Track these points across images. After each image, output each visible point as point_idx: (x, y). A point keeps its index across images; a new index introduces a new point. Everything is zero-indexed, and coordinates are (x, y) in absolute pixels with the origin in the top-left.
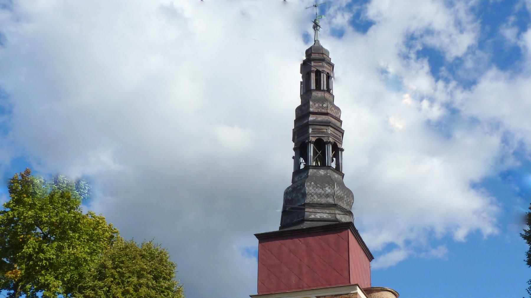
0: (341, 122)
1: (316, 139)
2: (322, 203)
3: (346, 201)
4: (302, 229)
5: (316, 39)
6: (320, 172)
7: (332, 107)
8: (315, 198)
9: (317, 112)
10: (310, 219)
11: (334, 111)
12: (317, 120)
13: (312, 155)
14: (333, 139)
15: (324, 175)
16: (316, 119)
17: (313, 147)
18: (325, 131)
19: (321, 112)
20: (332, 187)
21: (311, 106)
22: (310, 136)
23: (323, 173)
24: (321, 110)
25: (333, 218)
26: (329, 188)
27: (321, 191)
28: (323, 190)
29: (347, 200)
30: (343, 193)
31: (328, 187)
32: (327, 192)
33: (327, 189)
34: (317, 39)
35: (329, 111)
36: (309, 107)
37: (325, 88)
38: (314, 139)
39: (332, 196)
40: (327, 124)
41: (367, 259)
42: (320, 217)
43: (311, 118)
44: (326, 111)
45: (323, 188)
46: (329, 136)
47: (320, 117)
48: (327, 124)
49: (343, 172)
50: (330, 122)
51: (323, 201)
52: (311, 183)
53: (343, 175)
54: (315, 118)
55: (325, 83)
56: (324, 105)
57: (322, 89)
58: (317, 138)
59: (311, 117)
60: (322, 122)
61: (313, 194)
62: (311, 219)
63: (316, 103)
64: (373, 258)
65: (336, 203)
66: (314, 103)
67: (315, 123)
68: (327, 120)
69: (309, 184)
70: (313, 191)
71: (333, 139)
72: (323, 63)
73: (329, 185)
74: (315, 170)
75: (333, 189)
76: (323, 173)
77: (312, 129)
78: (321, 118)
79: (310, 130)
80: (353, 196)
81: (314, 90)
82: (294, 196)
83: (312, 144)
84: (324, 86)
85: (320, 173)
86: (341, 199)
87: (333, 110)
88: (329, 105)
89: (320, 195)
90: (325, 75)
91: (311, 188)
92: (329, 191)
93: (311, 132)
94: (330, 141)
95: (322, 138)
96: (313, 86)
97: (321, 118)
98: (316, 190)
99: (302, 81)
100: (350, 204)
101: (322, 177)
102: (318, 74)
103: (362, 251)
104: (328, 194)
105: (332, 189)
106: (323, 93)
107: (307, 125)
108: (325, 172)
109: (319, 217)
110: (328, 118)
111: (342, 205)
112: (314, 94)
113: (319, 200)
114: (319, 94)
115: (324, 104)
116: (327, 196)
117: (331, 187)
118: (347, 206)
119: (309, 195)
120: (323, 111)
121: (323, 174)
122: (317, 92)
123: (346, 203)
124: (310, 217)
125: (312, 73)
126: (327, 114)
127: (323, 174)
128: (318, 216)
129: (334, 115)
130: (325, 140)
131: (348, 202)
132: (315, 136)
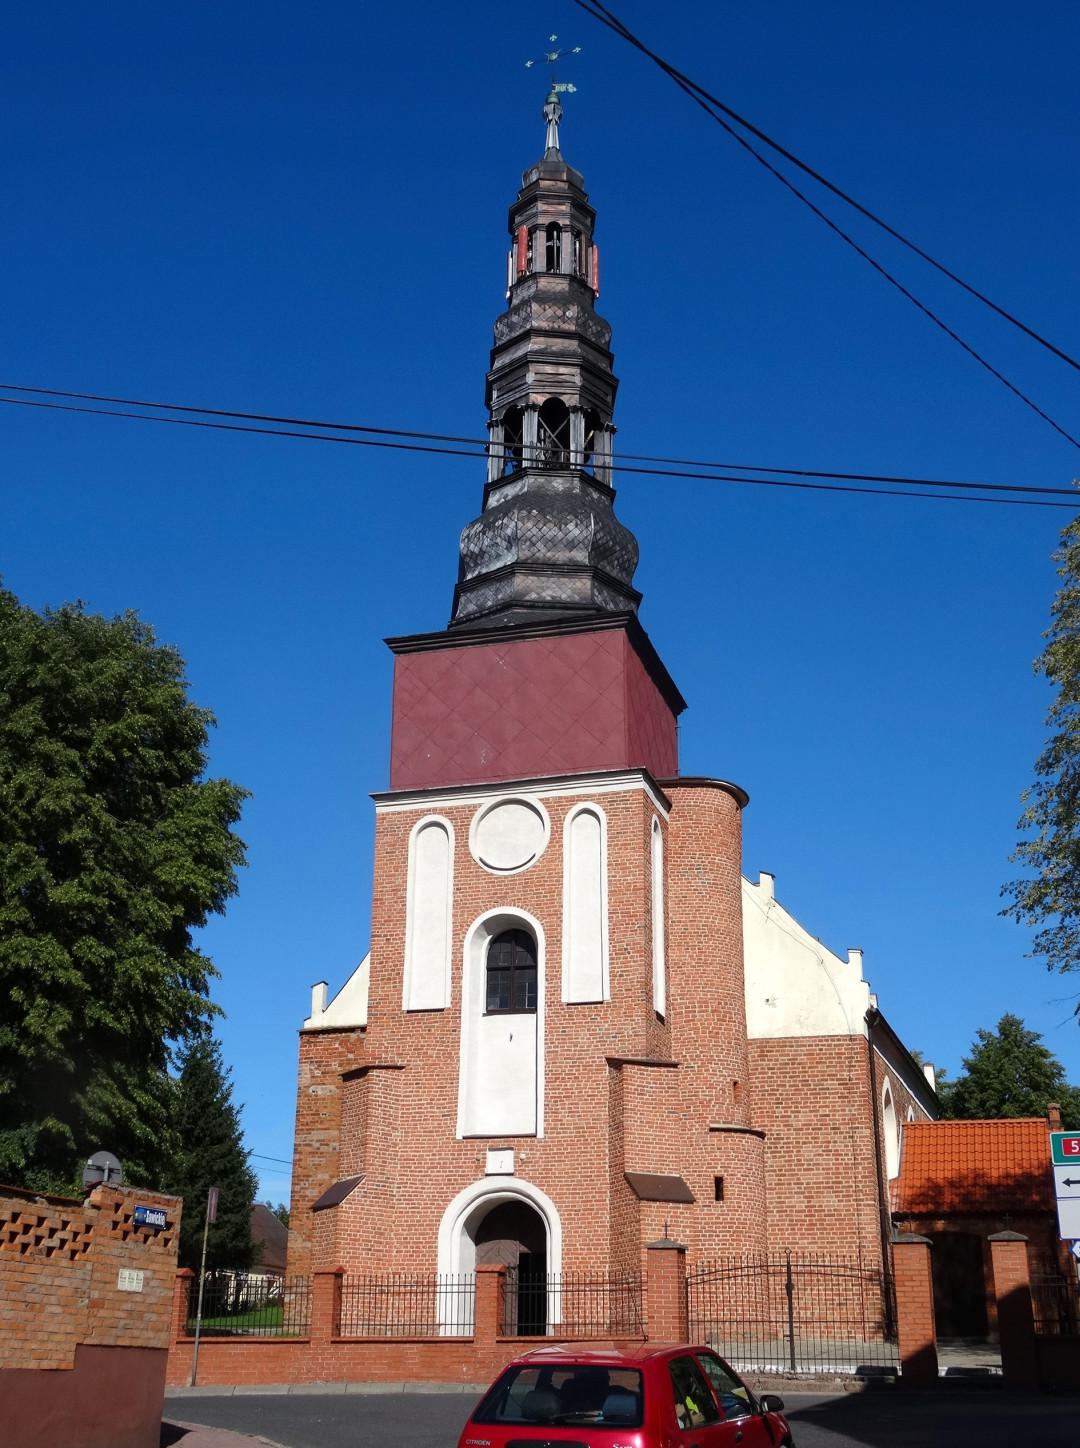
0: (610, 358)
2: (558, 563)
10: (526, 604)
23: (561, 488)
26: (576, 526)
28: (560, 529)
29: (622, 556)
30: (611, 539)
32: (570, 536)
33: (571, 526)
42: (553, 597)
45: (561, 523)
51: (562, 556)
52: (530, 512)
61: (534, 539)
70: (535, 531)
73: (576, 517)
74: (541, 480)
75: (587, 527)
76: (561, 488)
80: (636, 548)
82: (486, 543)
89: (552, 543)
92: (577, 532)
100: (629, 568)
108: (568, 485)
116: (571, 545)
117: (582, 523)
118: (621, 571)
119: (525, 542)
123: (619, 564)
124: (527, 598)
128: (547, 595)
131: (624, 562)
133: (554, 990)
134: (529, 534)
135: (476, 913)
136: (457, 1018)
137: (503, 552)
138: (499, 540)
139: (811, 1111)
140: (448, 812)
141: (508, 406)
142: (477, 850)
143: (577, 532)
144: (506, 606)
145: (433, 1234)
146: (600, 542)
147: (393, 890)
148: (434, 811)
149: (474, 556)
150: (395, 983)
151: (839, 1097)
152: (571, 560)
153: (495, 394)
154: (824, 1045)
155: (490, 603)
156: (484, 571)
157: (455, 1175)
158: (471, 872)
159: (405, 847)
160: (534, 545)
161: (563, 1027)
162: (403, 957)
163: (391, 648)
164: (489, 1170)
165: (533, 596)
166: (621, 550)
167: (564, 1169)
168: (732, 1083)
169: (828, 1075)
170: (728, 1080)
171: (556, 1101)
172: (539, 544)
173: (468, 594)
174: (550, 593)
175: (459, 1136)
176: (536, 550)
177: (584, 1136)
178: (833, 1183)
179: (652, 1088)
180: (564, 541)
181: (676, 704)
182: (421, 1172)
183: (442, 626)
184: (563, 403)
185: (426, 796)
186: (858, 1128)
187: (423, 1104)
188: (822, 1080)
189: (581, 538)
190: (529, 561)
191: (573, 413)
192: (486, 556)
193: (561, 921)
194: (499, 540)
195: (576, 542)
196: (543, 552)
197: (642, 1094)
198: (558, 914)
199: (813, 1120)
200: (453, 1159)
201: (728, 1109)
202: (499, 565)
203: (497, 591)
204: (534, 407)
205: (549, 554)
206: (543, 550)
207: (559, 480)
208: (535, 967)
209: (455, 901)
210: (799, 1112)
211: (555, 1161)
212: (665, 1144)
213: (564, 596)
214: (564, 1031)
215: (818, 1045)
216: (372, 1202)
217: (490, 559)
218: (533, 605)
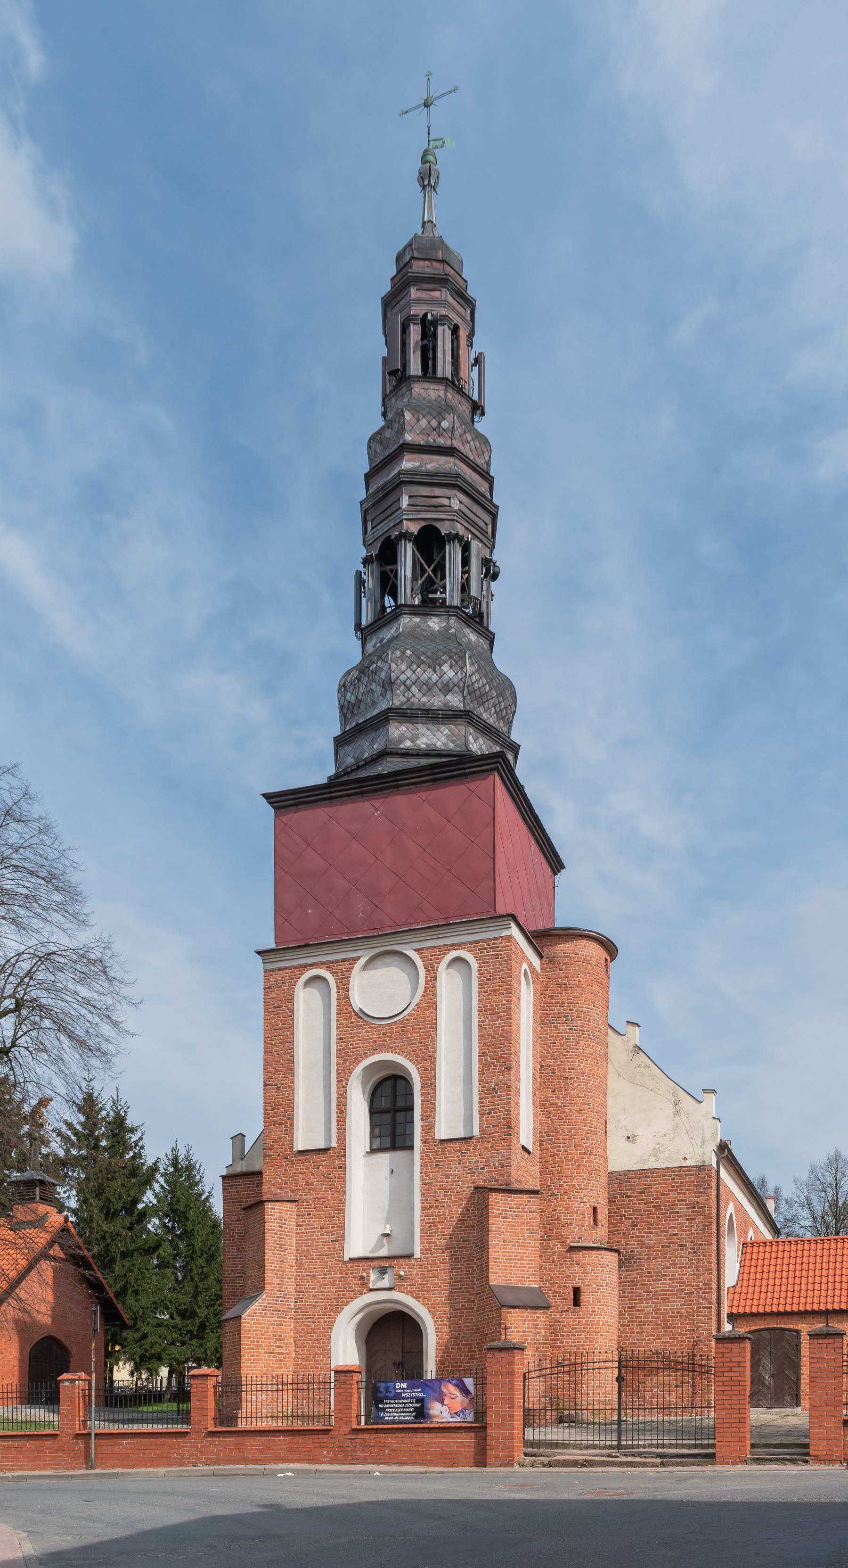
0: (490, 480)
1: (419, 527)
2: (433, 708)
3: (495, 706)
4: (380, 776)
5: (426, 219)
6: (431, 624)
7: (465, 433)
8: (414, 695)
9: (424, 444)
10: (400, 751)
11: (472, 443)
12: (423, 469)
13: (409, 573)
14: (466, 528)
15: (438, 631)
16: (420, 466)
17: (413, 551)
18: (445, 502)
19: (436, 445)
20: (460, 663)
21: (408, 427)
22: (404, 517)
23: (437, 628)
24: (434, 441)
25: (458, 749)
26: (451, 667)
27: (428, 675)
28: (435, 672)
29: (499, 703)
30: (487, 683)
31: (449, 662)
33: (445, 667)
34: (431, 219)
35: (456, 444)
36: (402, 431)
37: (448, 374)
38: (414, 528)
39: (459, 688)
40: (452, 482)
41: (549, 870)
42: (427, 745)
43: (408, 463)
44: (448, 443)
46: (455, 518)
47: (432, 461)
48: (452, 482)
49: (492, 628)
50: (458, 476)
51: (436, 701)
52: (403, 653)
53: (490, 638)
54: (417, 464)
55: (449, 358)
56: (443, 424)
57: (439, 374)
58: (423, 524)
59: (408, 461)
60: (436, 474)
62: (403, 751)
63: (421, 416)
64: (563, 867)
65: (468, 708)
66: (416, 416)
67: (417, 479)
68: (450, 468)
69: (398, 653)
70: (409, 673)
71: (466, 528)
72: (443, 289)
73: (451, 658)
74: (417, 620)
75: (462, 668)
76: (437, 628)
77: (410, 497)
78: (434, 463)
79: (405, 501)
80: (514, 694)
81: (418, 377)
83: (410, 541)
84: (444, 368)
85: (429, 627)
86: (481, 698)
87: (468, 442)
88: (457, 425)
89: (427, 687)
90: (448, 333)
91: (403, 667)
93: (408, 505)
94: (457, 534)
95: (438, 525)
96: (415, 367)
97: (434, 463)
98: (417, 672)
99: (386, 355)
100: (508, 716)
101: (432, 636)
102: (429, 328)
103: (533, 842)
104: (446, 685)
105: (458, 669)
106: (442, 388)
107: (397, 484)
109: (423, 746)
110: (455, 465)
111: (485, 716)
112: (418, 389)
113: (424, 699)
114: (431, 392)
115: (444, 419)
116: (446, 689)
117: (456, 663)
118: (498, 720)
119: (400, 686)
120: (441, 441)
121: (436, 629)
122: (426, 385)
123: (496, 713)
124: (402, 746)
125: (411, 325)
126: (450, 451)
127: (436, 629)
128: (422, 743)
129: (472, 458)
130: (444, 529)
131: (501, 710)
132: (419, 516)
133: (429, 1127)
134: (403, 677)
135: (357, 1061)
136: (342, 1156)
138: (374, 686)
139: (661, 1232)
140: (328, 965)
142: (358, 1001)
143: (451, 674)
144: (383, 754)
145: (326, 1339)
146: (476, 686)
147: (282, 1042)
150: (287, 1126)
151: (687, 1219)
152: (446, 704)
154: (676, 1175)
155: (366, 755)
156: (361, 721)
157: (344, 1291)
158: (352, 1023)
159: (291, 1000)
160: (409, 689)
161: (437, 1161)
162: (293, 1103)
163: (270, 803)
164: (371, 1286)
165: (408, 744)
166: (497, 696)
167: (438, 1283)
168: (592, 1208)
169: (678, 1201)
170: (588, 1206)
171: (430, 1226)
172: (414, 689)
174: (424, 740)
175: (346, 1259)
176: (411, 695)
177: (455, 1255)
178: (677, 1290)
179: (515, 1212)
180: (439, 684)
181: (556, 864)
182: (314, 1289)
183: (320, 778)
186: (702, 1244)
187: (315, 1232)
188: (673, 1205)
189: (456, 680)
190: (404, 707)
192: (362, 706)
193: (435, 1065)
195: (451, 685)
196: (420, 698)
197: (506, 1218)
198: (433, 1059)
199: (663, 1239)
200: (342, 1277)
201: (586, 1230)
202: (375, 712)
203: (372, 744)
204: (405, 536)
205: (424, 699)
206: (418, 695)
207: (436, 620)
208: (411, 1109)
210: (652, 1233)
211: (430, 1277)
212: (526, 1260)
213: (439, 744)
214: (438, 1165)
215: (671, 1175)
216: (272, 1314)
217: (366, 708)
218: (407, 754)
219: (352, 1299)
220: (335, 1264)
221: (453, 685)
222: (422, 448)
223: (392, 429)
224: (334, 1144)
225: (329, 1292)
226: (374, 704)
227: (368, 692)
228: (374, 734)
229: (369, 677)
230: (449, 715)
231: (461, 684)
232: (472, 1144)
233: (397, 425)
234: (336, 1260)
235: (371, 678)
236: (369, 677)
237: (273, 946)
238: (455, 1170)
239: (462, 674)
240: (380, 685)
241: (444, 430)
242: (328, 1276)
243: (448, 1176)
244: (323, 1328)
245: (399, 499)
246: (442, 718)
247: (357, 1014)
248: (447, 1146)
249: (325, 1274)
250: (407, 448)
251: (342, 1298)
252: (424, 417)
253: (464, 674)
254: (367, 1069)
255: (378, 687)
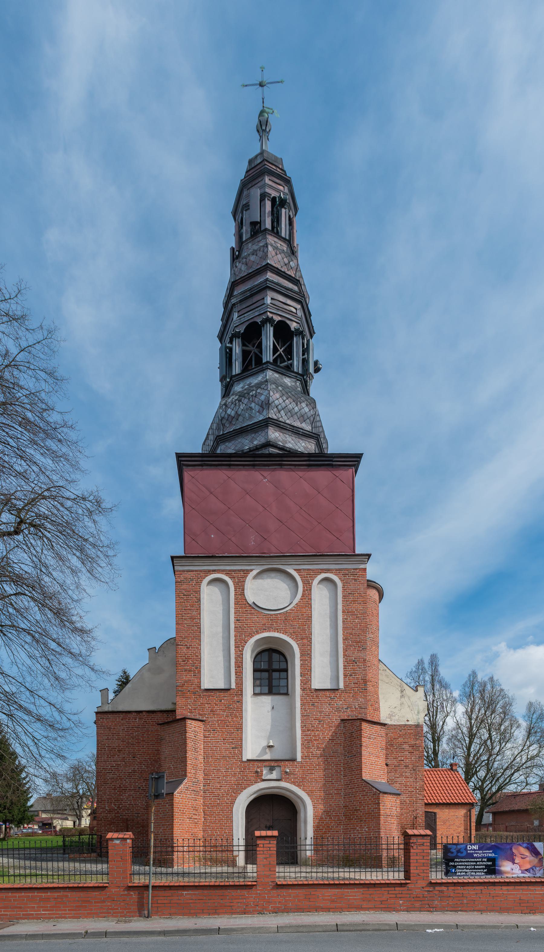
20: (312, 404)
31: (305, 402)
33: (304, 405)
39: (310, 421)
82: (242, 407)
89: (291, 413)
137: (255, 414)
141: (248, 323)
143: (306, 409)
148: (218, 571)
149: (230, 419)
153: (235, 315)
173: (227, 444)
184: (288, 327)
185: (215, 561)
189: (309, 415)
191: (296, 335)
194: (253, 405)
195: (306, 417)
209: (235, 627)
216: (191, 793)
219: (249, 785)
220: (235, 763)
221: (307, 418)
222: (280, 272)
223: (256, 255)
224: (233, 686)
225: (231, 780)
226: (251, 417)
227: (247, 409)
228: (253, 435)
229: (249, 399)
230: (306, 434)
231: (312, 419)
232: (338, 694)
233: (261, 253)
234: (236, 760)
235: (251, 399)
236: (249, 399)
237: (183, 554)
238: (326, 709)
239: (313, 412)
240: (258, 405)
241: (291, 268)
242: (230, 770)
243: (321, 712)
244: (227, 803)
245: (264, 298)
246: (301, 435)
247: (250, 606)
248: (321, 693)
249: (228, 769)
250: (268, 267)
251: (242, 785)
252: (280, 253)
253: (314, 413)
254: (258, 641)
255: (257, 406)
